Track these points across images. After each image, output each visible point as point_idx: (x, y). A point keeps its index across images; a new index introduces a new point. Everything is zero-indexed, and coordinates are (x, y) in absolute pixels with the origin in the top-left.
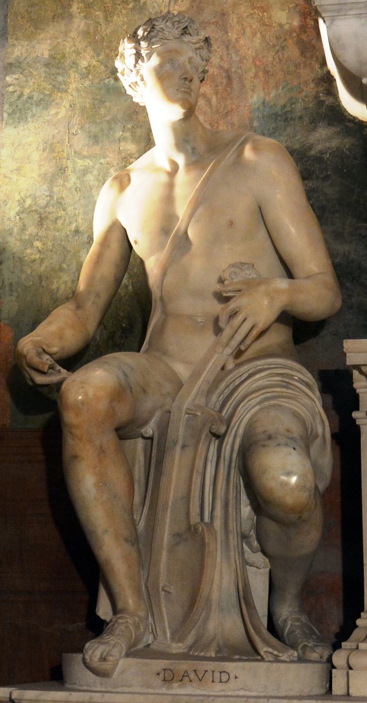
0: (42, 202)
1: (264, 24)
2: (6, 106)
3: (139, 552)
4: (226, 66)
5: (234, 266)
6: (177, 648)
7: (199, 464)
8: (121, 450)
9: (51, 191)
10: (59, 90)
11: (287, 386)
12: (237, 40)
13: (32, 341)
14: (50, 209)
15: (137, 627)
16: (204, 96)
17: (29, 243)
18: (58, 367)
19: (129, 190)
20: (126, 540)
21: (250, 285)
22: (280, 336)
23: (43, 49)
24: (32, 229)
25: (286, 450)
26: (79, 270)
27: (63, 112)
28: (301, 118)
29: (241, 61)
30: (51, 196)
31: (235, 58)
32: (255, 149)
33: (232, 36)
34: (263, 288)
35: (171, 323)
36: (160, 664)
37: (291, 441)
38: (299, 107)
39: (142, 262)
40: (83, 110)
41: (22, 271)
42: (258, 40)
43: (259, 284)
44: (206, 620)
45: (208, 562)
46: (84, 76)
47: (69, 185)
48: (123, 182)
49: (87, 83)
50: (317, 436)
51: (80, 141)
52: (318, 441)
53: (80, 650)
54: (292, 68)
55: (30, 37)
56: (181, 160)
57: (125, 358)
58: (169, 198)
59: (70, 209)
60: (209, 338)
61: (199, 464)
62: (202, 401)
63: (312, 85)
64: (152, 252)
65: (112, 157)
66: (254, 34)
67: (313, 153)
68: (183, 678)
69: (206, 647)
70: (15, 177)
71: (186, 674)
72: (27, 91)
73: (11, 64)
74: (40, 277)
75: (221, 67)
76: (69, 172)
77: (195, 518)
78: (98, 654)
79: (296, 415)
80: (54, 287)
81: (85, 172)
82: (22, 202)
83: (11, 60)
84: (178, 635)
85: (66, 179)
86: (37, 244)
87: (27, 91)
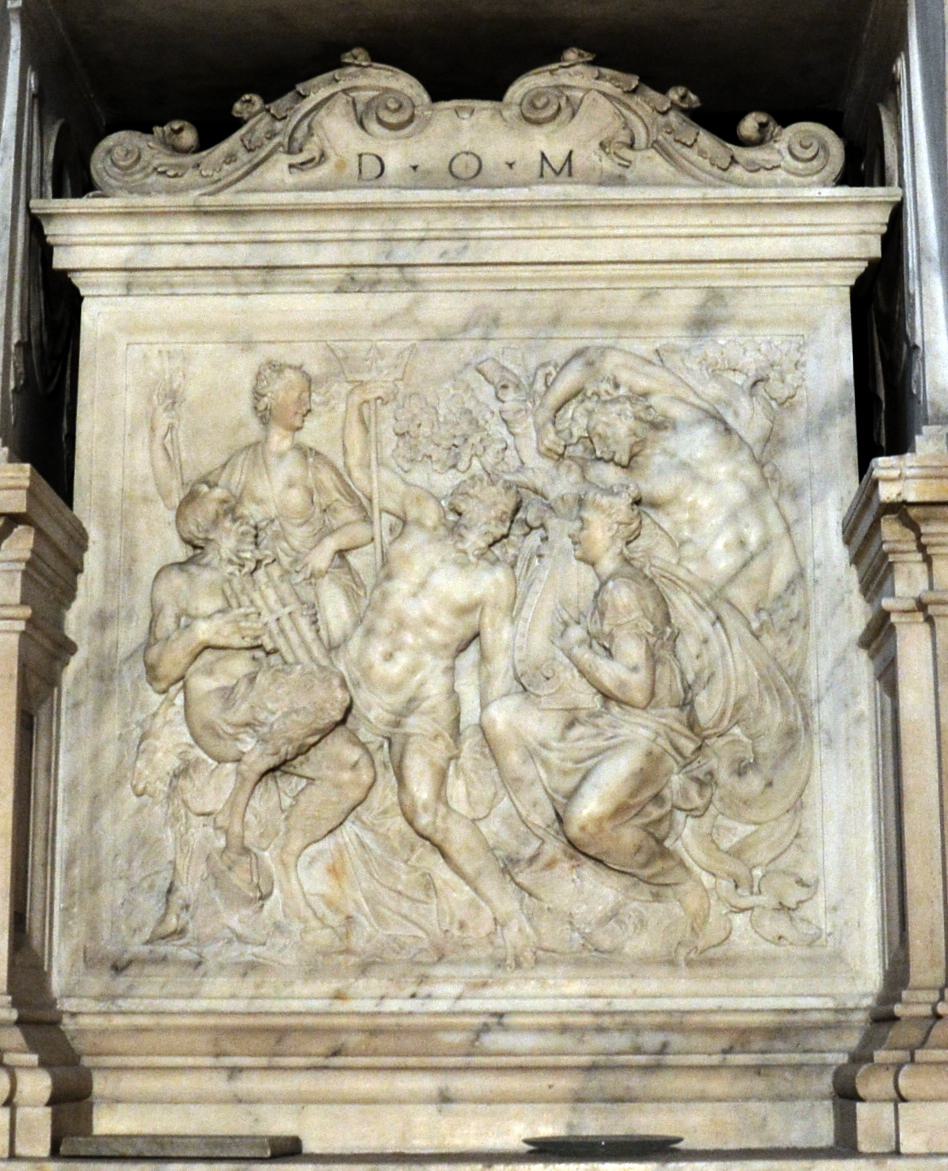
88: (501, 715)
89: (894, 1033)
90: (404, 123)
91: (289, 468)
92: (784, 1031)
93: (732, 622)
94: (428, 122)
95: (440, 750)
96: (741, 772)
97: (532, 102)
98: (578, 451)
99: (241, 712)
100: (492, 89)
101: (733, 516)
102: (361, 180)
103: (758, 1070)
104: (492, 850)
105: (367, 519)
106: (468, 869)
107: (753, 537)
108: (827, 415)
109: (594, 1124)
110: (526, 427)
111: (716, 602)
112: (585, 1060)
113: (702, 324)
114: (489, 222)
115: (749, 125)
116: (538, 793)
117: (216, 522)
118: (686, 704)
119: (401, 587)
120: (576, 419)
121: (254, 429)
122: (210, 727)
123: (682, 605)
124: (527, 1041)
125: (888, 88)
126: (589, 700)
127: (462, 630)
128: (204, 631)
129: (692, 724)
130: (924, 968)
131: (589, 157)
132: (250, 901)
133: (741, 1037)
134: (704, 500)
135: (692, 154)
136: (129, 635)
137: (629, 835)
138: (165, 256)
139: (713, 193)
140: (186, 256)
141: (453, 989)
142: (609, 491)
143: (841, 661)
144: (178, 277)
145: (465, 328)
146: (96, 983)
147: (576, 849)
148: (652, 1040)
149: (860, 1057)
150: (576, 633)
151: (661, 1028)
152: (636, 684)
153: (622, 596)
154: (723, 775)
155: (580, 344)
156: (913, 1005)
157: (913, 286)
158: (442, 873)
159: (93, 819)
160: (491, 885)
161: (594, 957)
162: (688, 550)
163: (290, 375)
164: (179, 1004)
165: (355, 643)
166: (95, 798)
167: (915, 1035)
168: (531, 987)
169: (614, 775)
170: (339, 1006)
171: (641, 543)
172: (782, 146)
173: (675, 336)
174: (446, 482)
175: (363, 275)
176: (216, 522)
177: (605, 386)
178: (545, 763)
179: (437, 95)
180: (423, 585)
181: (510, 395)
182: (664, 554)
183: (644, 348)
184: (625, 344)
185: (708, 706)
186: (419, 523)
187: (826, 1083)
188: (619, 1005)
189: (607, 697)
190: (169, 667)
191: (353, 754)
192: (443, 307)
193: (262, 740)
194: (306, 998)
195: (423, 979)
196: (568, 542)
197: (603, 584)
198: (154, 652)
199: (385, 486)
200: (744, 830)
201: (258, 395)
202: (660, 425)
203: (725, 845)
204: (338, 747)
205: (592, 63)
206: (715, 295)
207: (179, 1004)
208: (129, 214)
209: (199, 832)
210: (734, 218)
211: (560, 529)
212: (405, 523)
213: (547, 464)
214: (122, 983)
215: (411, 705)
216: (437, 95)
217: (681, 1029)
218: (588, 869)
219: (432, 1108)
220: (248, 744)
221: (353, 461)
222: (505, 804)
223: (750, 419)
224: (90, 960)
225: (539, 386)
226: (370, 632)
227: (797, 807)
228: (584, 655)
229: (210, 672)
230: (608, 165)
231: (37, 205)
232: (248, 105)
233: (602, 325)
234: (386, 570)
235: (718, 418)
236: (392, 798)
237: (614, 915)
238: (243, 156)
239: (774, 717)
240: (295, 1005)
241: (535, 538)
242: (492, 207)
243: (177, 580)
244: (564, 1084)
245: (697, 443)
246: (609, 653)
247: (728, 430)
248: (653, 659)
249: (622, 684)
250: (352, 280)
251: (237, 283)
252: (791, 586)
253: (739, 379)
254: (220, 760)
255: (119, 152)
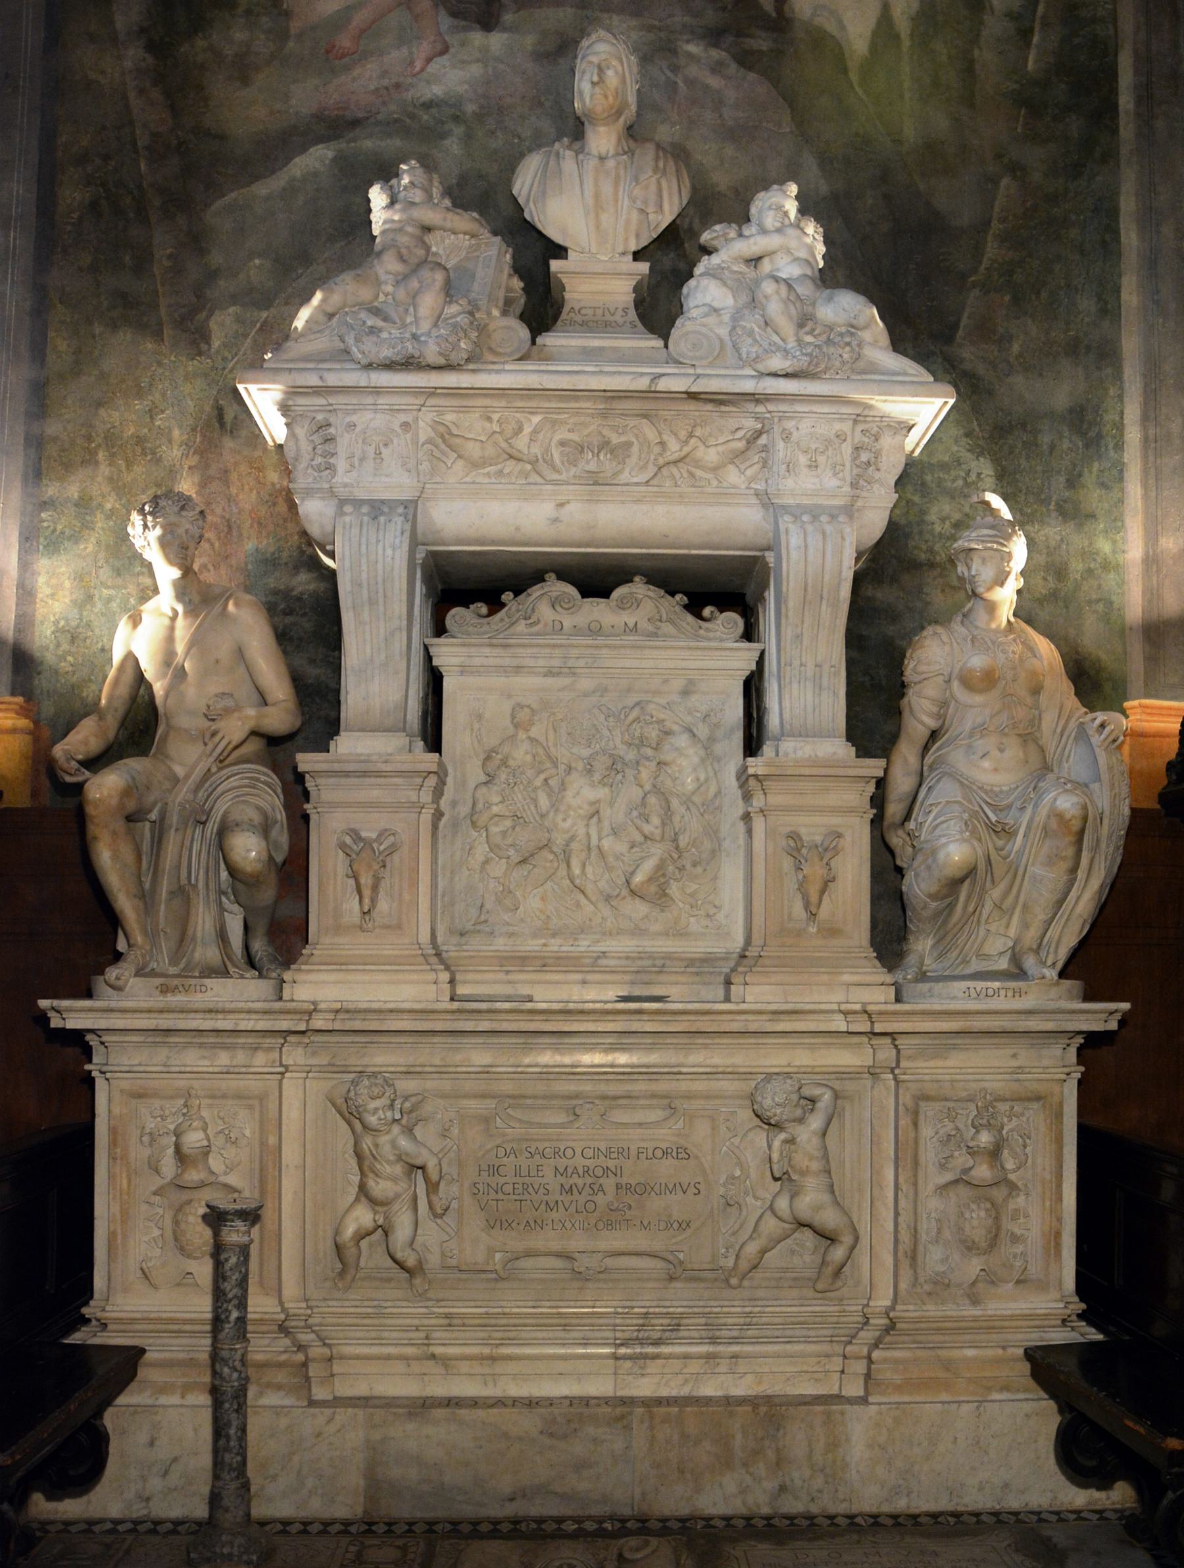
0: (74, 623)
1: (259, 483)
2: (42, 540)
3: (145, 903)
4: (227, 516)
5: (216, 696)
6: (172, 970)
7: (187, 843)
8: (130, 833)
9: (81, 615)
10: (87, 528)
11: (254, 787)
12: (237, 495)
13: (63, 750)
14: (80, 630)
15: (144, 956)
16: (209, 540)
17: (63, 658)
18: (83, 770)
19: (140, 628)
20: (135, 896)
21: (228, 711)
22: (254, 746)
23: (73, 491)
24: (65, 646)
25: (247, 834)
26: (104, 682)
27: (90, 548)
28: (286, 564)
29: (239, 513)
30: (81, 619)
31: (235, 510)
32: (236, 604)
33: (234, 491)
34: (236, 714)
35: (172, 733)
36: (158, 981)
37: (252, 827)
38: (285, 554)
39: (151, 686)
40: (108, 546)
41: (58, 681)
42: (254, 495)
43: (235, 710)
44: (193, 951)
45: (193, 911)
46: (109, 517)
47: (96, 610)
48: (136, 621)
49: (111, 523)
50: (276, 822)
51: (105, 573)
52: (278, 825)
53: (102, 973)
54: (281, 522)
55: (61, 479)
56: (180, 608)
57: (134, 764)
58: (170, 638)
59: (97, 631)
60: (201, 747)
61: (187, 843)
62: (191, 797)
63: (296, 537)
64: (158, 679)
65: (132, 589)
66: (251, 490)
67: (294, 593)
68: (174, 990)
69: (192, 970)
70: (50, 602)
71: (176, 987)
72: (59, 527)
73: (45, 503)
74: (73, 687)
75: (223, 517)
76: (96, 599)
77: (184, 881)
78: (114, 975)
79: (258, 808)
80: (84, 694)
81: (109, 600)
82: (56, 622)
83: (45, 499)
84: (174, 961)
85: (94, 605)
86: (70, 658)
87: (59, 527)
88: (606, 843)
89: (745, 961)
90: (571, 609)
91: (525, 746)
92: (708, 959)
93: (693, 809)
94: (580, 607)
95: (584, 855)
96: (694, 865)
97: (622, 599)
98: (637, 742)
99: (510, 841)
100: (605, 594)
101: (695, 770)
102: (554, 632)
103: (697, 974)
104: (601, 892)
105: (557, 767)
106: (593, 899)
107: (702, 777)
108: (732, 730)
109: (637, 992)
110: (617, 732)
111: (687, 802)
112: (635, 969)
113: (686, 693)
114: (604, 651)
115: (707, 612)
116: (620, 872)
117: (499, 767)
118: (675, 840)
119: (569, 794)
120: (637, 730)
121: (512, 728)
122: (498, 846)
123: (675, 803)
124: (612, 962)
125: (761, 599)
126: (640, 839)
127: (593, 809)
128: (495, 809)
129: (677, 848)
130: (757, 939)
131: (644, 625)
132: (512, 910)
133: (691, 962)
134: (684, 762)
135: (684, 624)
136: (464, 810)
137: (653, 889)
138: (477, 661)
139: (692, 644)
140: (485, 662)
141: (586, 943)
142: (648, 759)
143: (733, 825)
144: (482, 669)
145: (593, 692)
146: (455, 940)
147: (633, 893)
148: (659, 962)
149: (733, 970)
150: (635, 813)
151: (663, 958)
152: (658, 832)
153: (652, 800)
154: (688, 867)
155: (636, 700)
156: (752, 952)
157: (766, 684)
158: (584, 901)
159: (452, 879)
160: (601, 905)
161: (638, 932)
162: (678, 782)
163: (526, 709)
164: (484, 948)
165: (552, 814)
166: (452, 872)
167: (752, 962)
168: (614, 943)
169: (648, 867)
170: (545, 949)
171: (660, 779)
172: (719, 622)
173: (676, 698)
174: (586, 753)
175: (555, 670)
176: (499, 767)
177: (648, 717)
178: (623, 862)
179: (583, 597)
180: (578, 793)
181: (611, 719)
182: (669, 782)
183: (663, 701)
184: (655, 700)
185: (683, 841)
186: (576, 769)
187: (722, 979)
188: (648, 949)
189: (646, 837)
190: (481, 823)
191: (551, 857)
192: (585, 684)
193: (516, 851)
194: (533, 945)
195: (576, 939)
196: (632, 778)
197: (646, 795)
198: (475, 818)
199: (562, 754)
200: (695, 887)
201: (513, 717)
202: (668, 733)
203: (688, 891)
204: (545, 853)
205: (647, 583)
206: (691, 682)
207: (484, 948)
208: (463, 645)
209: (492, 884)
210: (699, 653)
211: (630, 773)
212: (570, 769)
213: (625, 747)
214: (464, 940)
215: (572, 838)
216: (585, 595)
217: (670, 958)
218: (637, 900)
219: (579, 986)
220: (512, 852)
221: (550, 744)
222: (607, 876)
223: (702, 731)
224: (451, 931)
225: (622, 717)
226: (557, 810)
227: (715, 878)
228: (639, 822)
229: (496, 825)
230: (651, 628)
231: (427, 641)
232: (507, 596)
233: (647, 692)
234: (563, 787)
235: (691, 731)
236: (565, 873)
237: (647, 916)
238: (507, 620)
239: (707, 845)
240: (529, 948)
241: (620, 776)
242: (606, 646)
243: (484, 789)
244: (628, 978)
245: (682, 741)
246: (647, 821)
247: (694, 735)
248: (664, 824)
249: (652, 833)
250: (550, 673)
251: (505, 672)
252: (716, 796)
253: (698, 715)
254: (500, 858)
255: (457, 618)
